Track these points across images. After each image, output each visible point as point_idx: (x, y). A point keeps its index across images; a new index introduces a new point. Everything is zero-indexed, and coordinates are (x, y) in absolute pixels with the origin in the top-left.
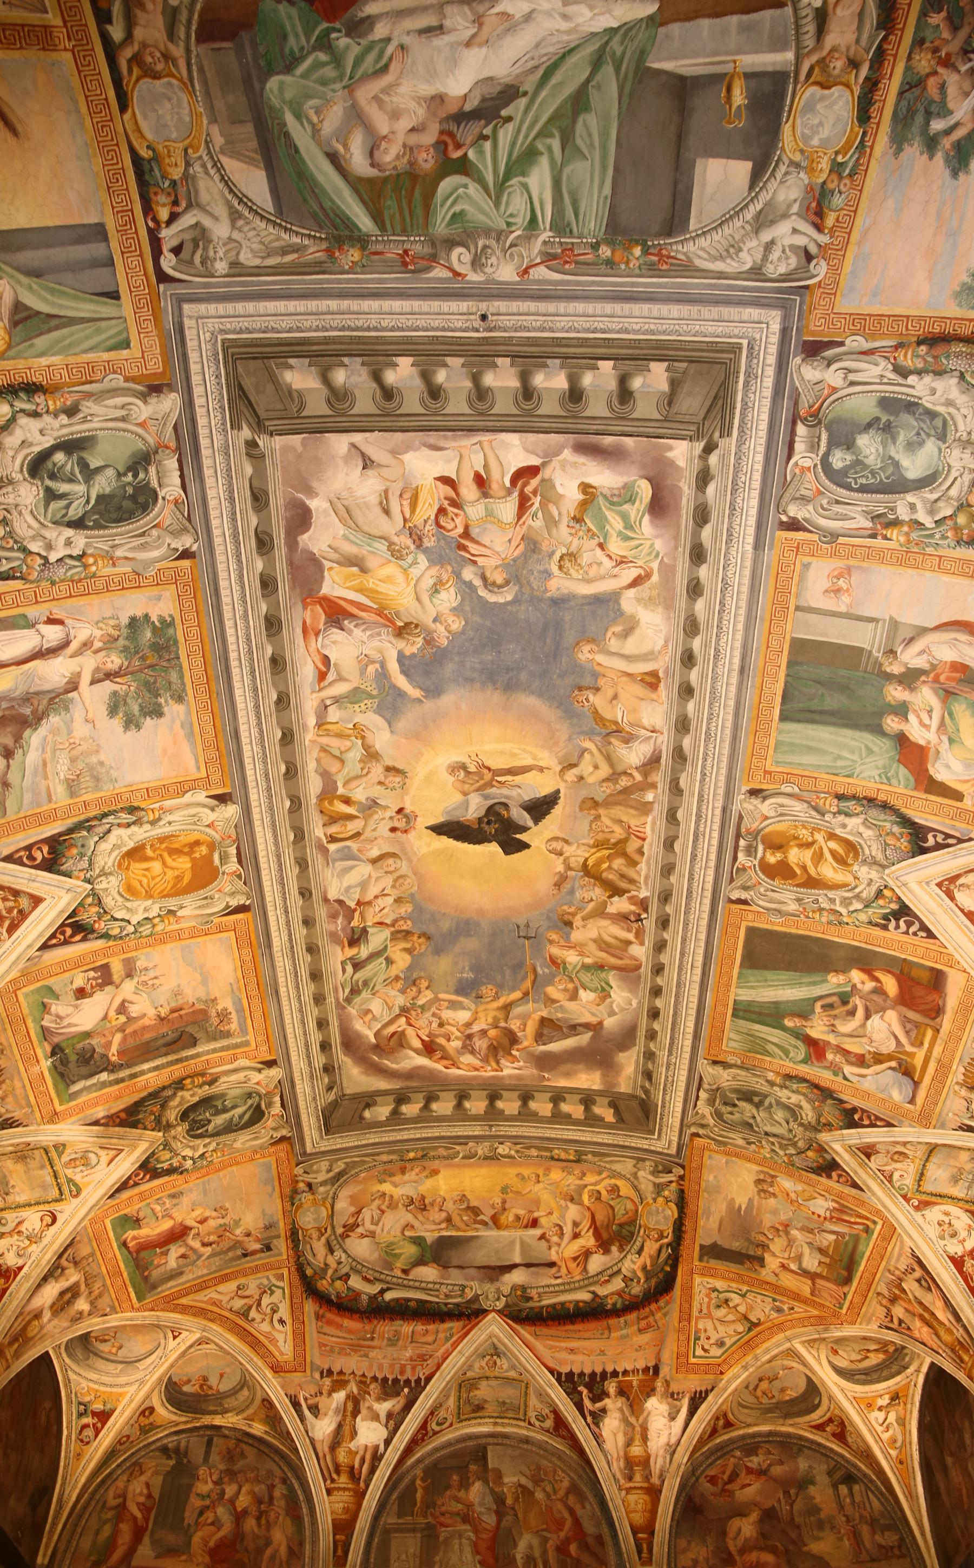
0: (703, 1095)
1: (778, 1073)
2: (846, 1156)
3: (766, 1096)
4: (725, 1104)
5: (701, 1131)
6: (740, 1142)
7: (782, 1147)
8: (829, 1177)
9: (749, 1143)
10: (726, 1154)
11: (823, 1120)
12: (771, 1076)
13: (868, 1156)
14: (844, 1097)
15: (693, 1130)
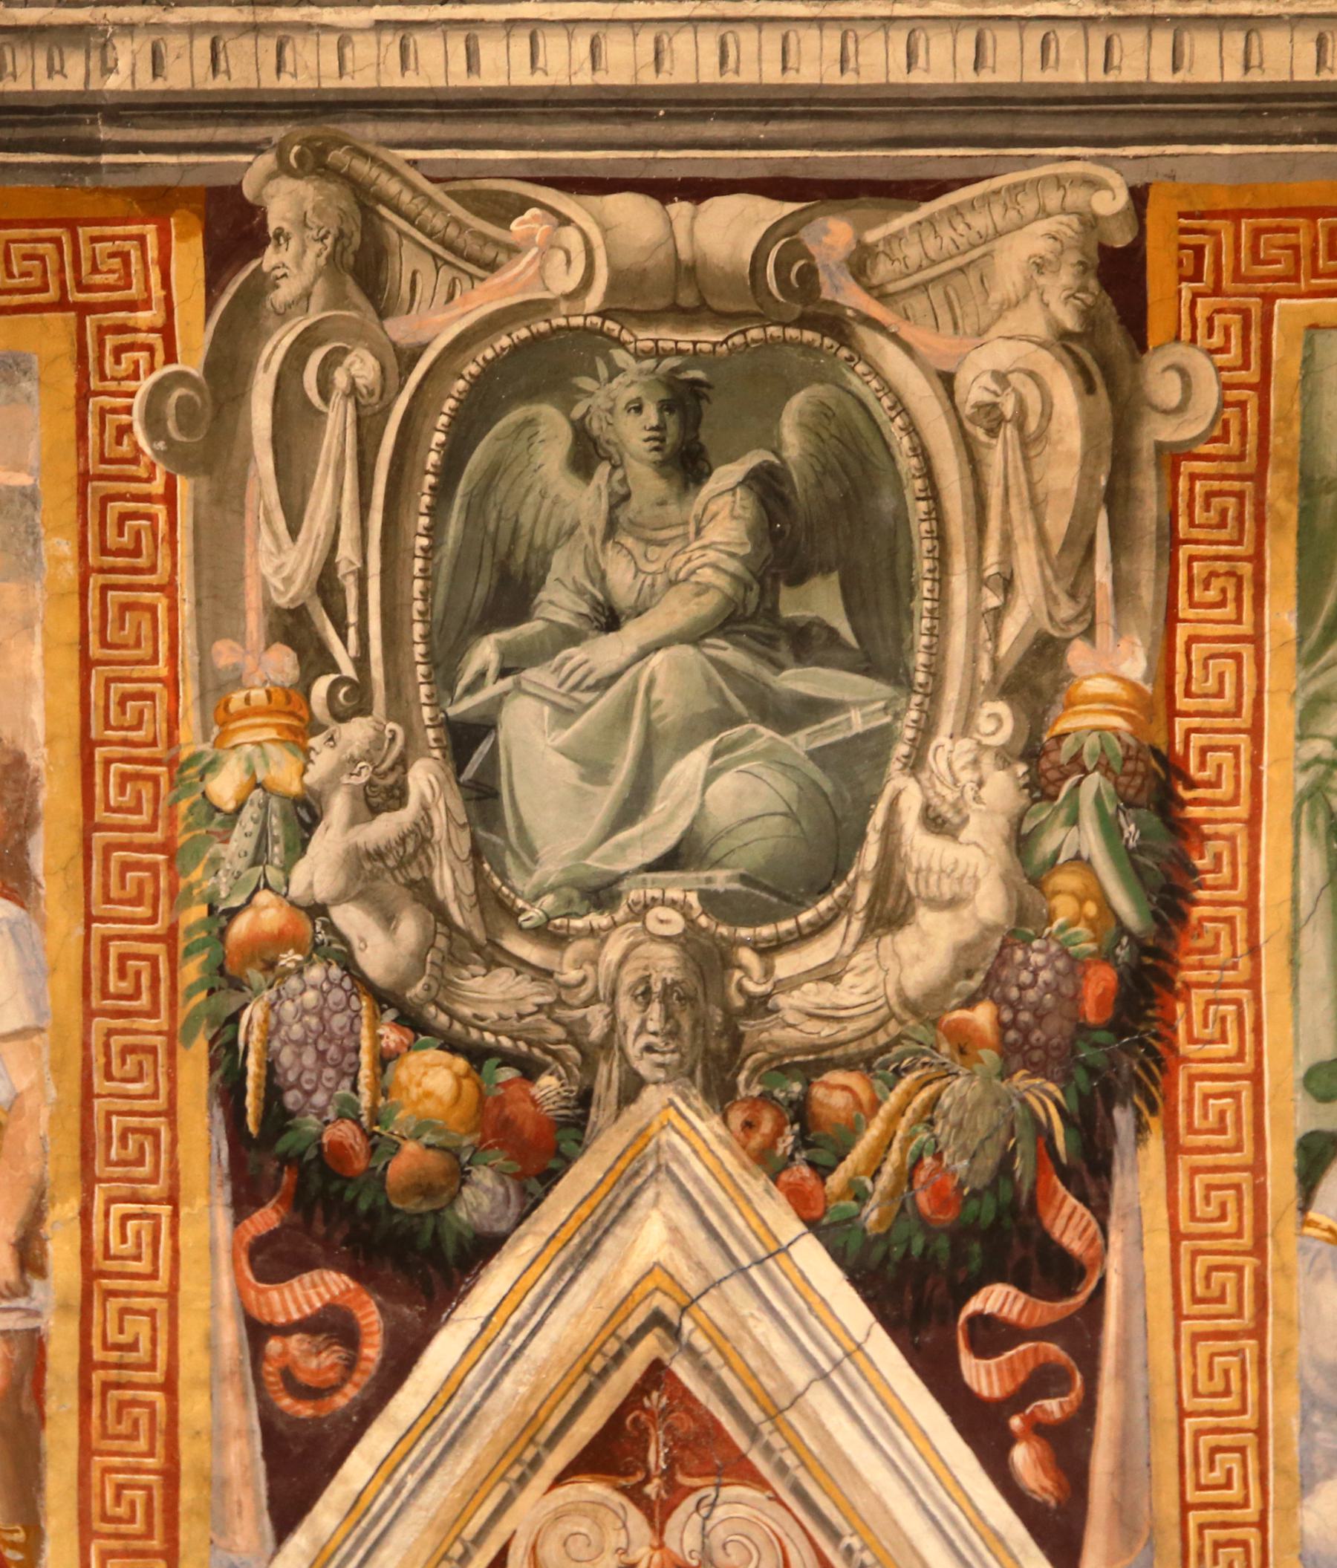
0: (730, 230)
1: (1159, 699)
2: (571, 1324)
3: (881, 659)
4: (684, 398)
5: (292, 266)
6: (278, 566)
7: (388, 875)
8: (272, 1260)
9: (291, 627)
10: (95, 484)
11: (835, 1094)
12: (1110, 668)
13: (608, 1456)
14: (1141, 1174)
15: (285, 202)
